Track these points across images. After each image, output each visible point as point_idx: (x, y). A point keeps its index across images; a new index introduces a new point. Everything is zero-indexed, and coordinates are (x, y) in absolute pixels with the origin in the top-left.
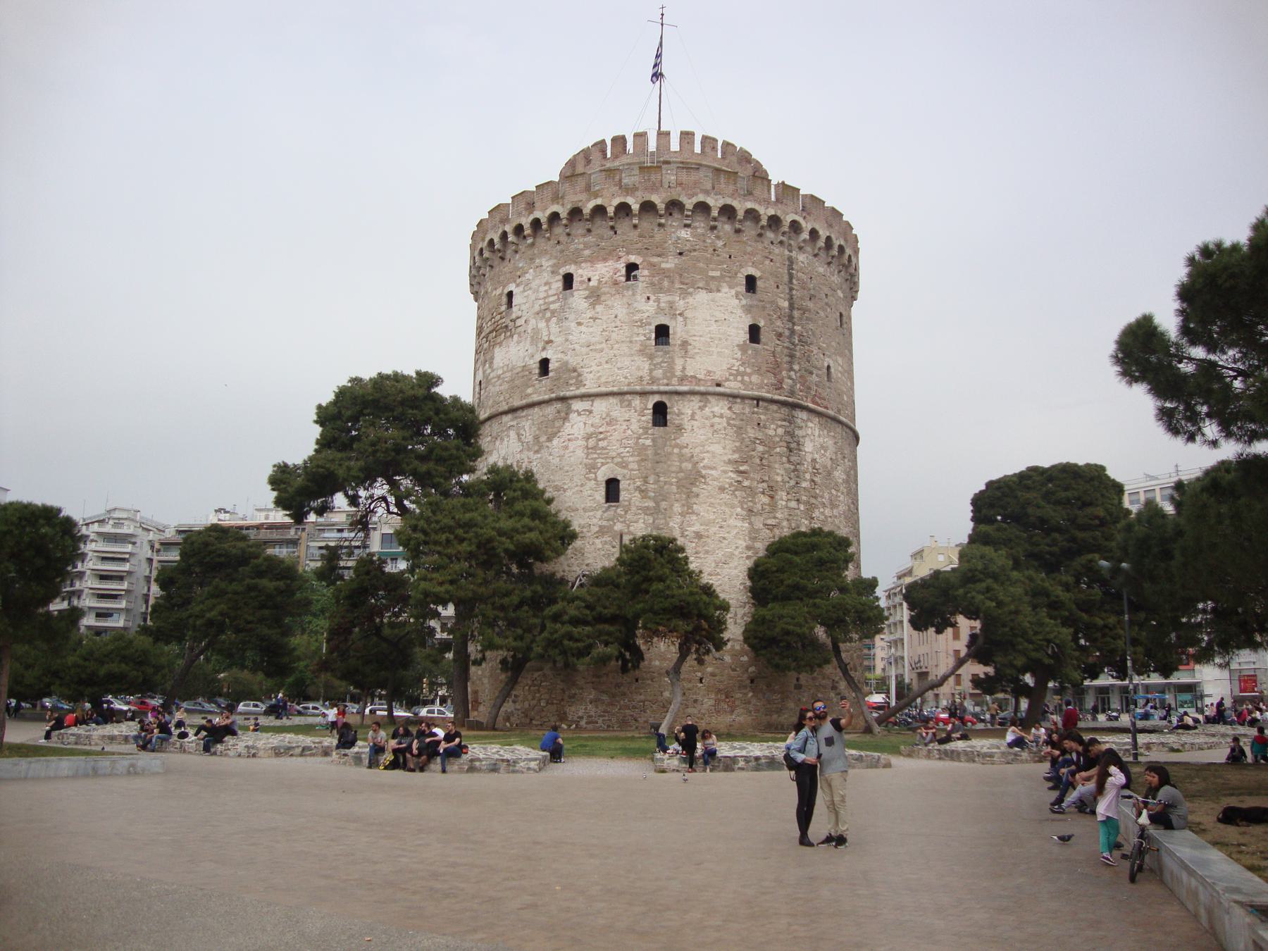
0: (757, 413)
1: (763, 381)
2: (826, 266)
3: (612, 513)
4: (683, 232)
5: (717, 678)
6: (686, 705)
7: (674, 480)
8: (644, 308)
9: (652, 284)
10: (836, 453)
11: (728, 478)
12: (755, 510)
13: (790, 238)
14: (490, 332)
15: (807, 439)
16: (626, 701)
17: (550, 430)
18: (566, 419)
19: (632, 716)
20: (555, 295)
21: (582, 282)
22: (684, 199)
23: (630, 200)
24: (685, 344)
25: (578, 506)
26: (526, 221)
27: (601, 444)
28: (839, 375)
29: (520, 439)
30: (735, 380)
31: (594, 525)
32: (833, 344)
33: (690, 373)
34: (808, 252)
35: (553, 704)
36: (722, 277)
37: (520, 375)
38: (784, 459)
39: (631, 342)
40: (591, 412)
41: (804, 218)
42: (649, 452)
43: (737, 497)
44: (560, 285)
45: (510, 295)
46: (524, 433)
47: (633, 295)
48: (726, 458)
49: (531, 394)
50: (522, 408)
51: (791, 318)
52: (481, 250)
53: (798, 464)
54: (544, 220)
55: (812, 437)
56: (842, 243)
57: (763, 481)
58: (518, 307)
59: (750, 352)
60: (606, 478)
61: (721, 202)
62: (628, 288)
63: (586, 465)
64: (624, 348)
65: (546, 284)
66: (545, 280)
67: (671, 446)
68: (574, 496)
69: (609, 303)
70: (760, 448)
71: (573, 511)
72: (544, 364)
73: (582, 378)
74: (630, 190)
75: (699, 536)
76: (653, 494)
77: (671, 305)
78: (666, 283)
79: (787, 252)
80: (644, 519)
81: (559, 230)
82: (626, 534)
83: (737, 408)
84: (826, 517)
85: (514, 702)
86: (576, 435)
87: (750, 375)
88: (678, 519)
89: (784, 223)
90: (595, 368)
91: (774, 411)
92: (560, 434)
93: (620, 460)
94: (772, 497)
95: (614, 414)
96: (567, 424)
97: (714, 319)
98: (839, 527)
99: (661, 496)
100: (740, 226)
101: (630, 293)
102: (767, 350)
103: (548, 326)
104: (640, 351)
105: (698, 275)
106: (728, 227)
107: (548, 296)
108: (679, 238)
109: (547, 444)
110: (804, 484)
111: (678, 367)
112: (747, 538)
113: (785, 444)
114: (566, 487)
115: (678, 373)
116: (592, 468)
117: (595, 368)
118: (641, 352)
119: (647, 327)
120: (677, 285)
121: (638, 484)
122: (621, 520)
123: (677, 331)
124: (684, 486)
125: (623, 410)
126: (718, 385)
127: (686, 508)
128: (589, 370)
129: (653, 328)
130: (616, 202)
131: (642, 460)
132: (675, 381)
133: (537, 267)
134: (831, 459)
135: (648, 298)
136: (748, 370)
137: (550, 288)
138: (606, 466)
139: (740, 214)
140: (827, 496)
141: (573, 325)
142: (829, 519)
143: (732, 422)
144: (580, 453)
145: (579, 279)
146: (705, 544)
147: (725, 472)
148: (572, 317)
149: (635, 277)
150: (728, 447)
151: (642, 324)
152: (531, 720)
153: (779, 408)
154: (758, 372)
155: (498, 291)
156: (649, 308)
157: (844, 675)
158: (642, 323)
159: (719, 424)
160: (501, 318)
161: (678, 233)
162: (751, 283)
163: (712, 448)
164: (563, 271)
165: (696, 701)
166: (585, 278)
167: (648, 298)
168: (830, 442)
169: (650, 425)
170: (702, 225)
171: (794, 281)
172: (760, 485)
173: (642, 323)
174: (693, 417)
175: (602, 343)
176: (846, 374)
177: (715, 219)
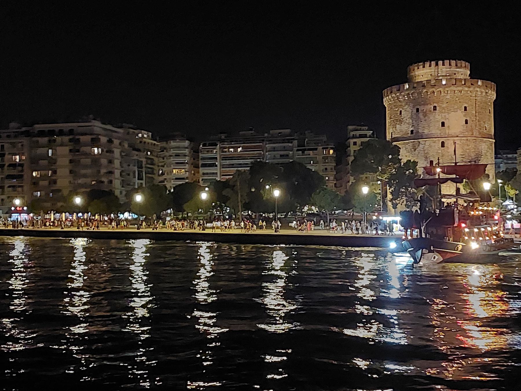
18: (419, 146)
21: (422, 110)
24: (449, 127)
33: (450, 133)
44: (415, 111)
45: (401, 111)
51: (476, 116)
62: (434, 112)
70: (468, 151)
77: (445, 116)
83: (462, 141)
87: (465, 132)
111: (447, 132)
118: (437, 129)
155: (397, 109)
162: (465, 109)
171: (477, 105)
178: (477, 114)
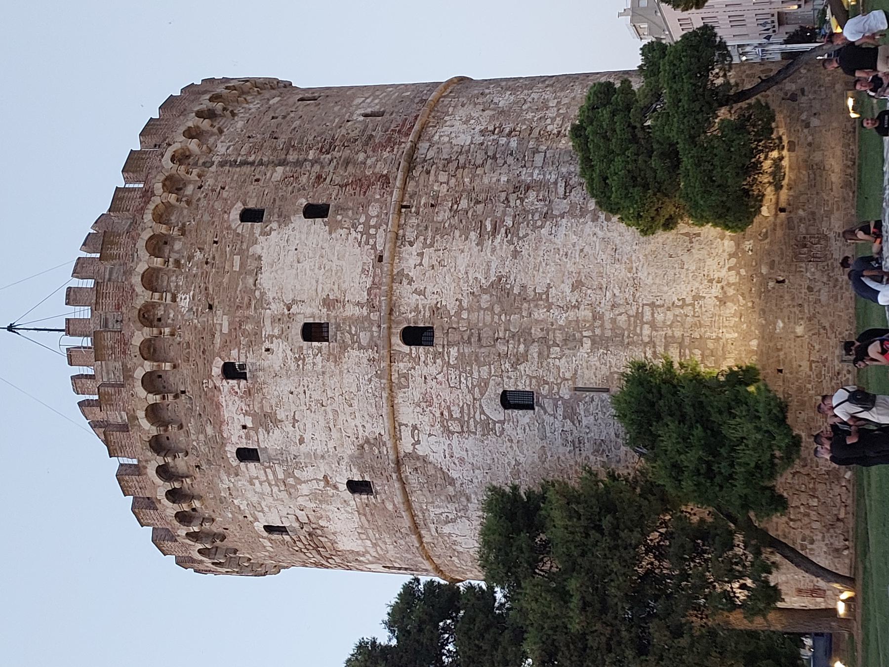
0: (418, 208)
1: (377, 201)
2: (236, 118)
3: (546, 400)
4: (182, 304)
5: (777, 259)
6: (815, 303)
7: (503, 317)
8: (281, 355)
9: (250, 344)
10: (476, 104)
11: (501, 249)
12: (546, 209)
13: (196, 164)
14: (319, 552)
15: (454, 142)
16: (809, 386)
17: (439, 481)
18: (425, 460)
19: (831, 379)
20: (265, 472)
21: (248, 437)
22: (139, 302)
23: (139, 373)
24: (328, 303)
25: (538, 447)
26: (170, 509)
27: (456, 415)
28: (377, 101)
29: (453, 521)
30: (375, 236)
31: (563, 426)
32: (336, 109)
34: (216, 141)
35: (814, 489)
36: (241, 253)
37: (371, 519)
38: (479, 171)
39: (324, 373)
40: (415, 427)
41: (169, 145)
42: (466, 351)
43: (527, 234)
44: (251, 465)
45: (269, 529)
46: (444, 515)
47: (263, 370)
48: (476, 249)
49: (394, 505)
50: (413, 516)
51: (299, 163)
52: (213, 563)
53: (486, 153)
54: (169, 486)
55: (453, 135)
56: (208, 97)
57: (507, 199)
58: (283, 519)
59: (339, 218)
60: (501, 409)
61: (144, 254)
62: (254, 377)
63: (483, 435)
64: (332, 382)
65: (252, 484)
66: (245, 483)
67: (458, 323)
68: (525, 452)
69: (273, 402)
70: (464, 204)
71: (546, 454)
72: (355, 487)
73: (371, 437)
74: (128, 373)
75: (577, 286)
76: (522, 347)
77: (278, 320)
78: (249, 327)
79: (213, 168)
80: (555, 358)
81: (181, 464)
82: (574, 383)
83: (410, 234)
84: (558, 115)
85: (812, 542)
86: (446, 447)
87: (369, 218)
88: (555, 311)
89: (173, 172)
90: (358, 421)
91: (417, 186)
92: (444, 467)
93: (476, 389)
94: (528, 188)
95: (417, 396)
96: (431, 459)
97: (295, 264)
98: (574, 98)
99: (524, 336)
100: (176, 228)
101: (261, 373)
102: (337, 196)
103: (304, 482)
104: (336, 361)
105: (238, 285)
106: (177, 246)
107: (268, 480)
108: (190, 309)
109: (458, 485)
110: (514, 143)
111: (357, 311)
112: (581, 221)
113: (461, 170)
114: (514, 463)
115: (365, 311)
116: (487, 427)
117: (358, 421)
118: (337, 361)
119: (305, 352)
120: (252, 313)
121: (507, 365)
122: (556, 389)
123: (311, 312)
124: (512, 305)
125: (411, 384)
126: (380, 259)
127: (541, 303)
128: (360, 429)
129: (306, 344)
130: (141, 392)
131: (476, 361)
132: (374, 316)
133: (230, 494)
134: (483, 110)
135: (267, 350)
136: (362, 220)
137: (257, 478)
138: (485, 408)
139: (163, 229)
140: (530, 116)
141: (303, 448)
142: (561, 111)
143: (428, 242)
144: (469, 442)
145: (244, 441)
146: (589, 276)
147: (493, 250)
148: (293, 449)
149: (243, 366)
150: (461, 247)
151: (300, 359)
152: (838, 520)
153: (413, 179)
154: (365, 206)
156: (281, 350)
157: (777, 83)
158: (300, 358)
159: (430, 258)
160: (300, 541)
161: (184, 311)
162: (251, 215)
163: (462, 269)
164: (234, 462)
165: (810, 289)
166: (243, 432)
167: (267, 350)
168: (462, 112)
169: (431, 349)
170: (174, 278)
171: (251, 159)
172: (512, 204)
173: (300, 358)
174: (421, 293)
175: (325, 410)
176: (377, 93)
177: (166, 262)
178: (292, 157)
